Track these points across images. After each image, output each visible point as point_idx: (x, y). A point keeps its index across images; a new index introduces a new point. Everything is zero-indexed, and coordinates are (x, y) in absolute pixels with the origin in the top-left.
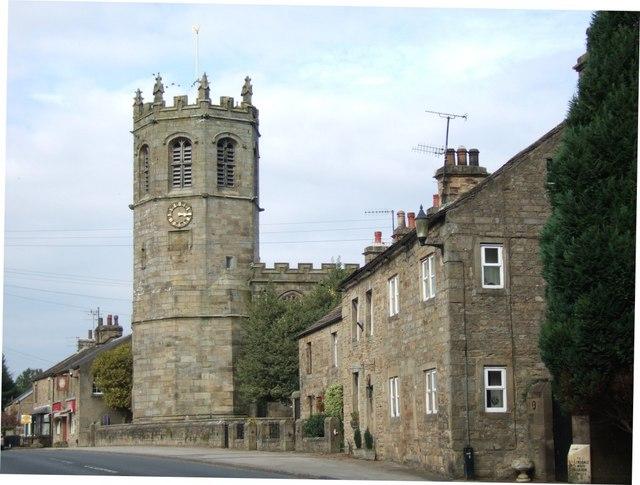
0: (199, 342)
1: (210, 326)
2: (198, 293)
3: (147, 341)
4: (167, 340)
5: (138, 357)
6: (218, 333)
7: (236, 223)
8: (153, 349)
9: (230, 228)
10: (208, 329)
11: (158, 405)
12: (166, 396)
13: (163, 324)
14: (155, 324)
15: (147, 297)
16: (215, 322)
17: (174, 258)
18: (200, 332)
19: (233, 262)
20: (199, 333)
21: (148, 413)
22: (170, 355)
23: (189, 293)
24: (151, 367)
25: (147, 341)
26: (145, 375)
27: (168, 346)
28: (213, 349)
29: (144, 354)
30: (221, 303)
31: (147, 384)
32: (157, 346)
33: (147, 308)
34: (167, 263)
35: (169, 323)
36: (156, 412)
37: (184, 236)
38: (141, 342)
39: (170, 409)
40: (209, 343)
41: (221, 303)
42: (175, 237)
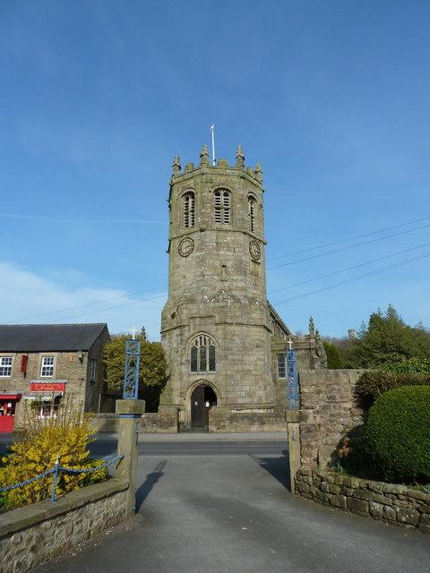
8: (244, 348)
11: (250, 395)
12: (257, 387)
15: (237, 305)
21: (240, 401)
24: (242, 362)
25: (237, 340)
26: (236, 367)
29: (235, 351)
31: (239, 376)
32: (247, 345)
33: (238, 314)
35: (258, 329)
36: (248, 400)
39: (260, 398)
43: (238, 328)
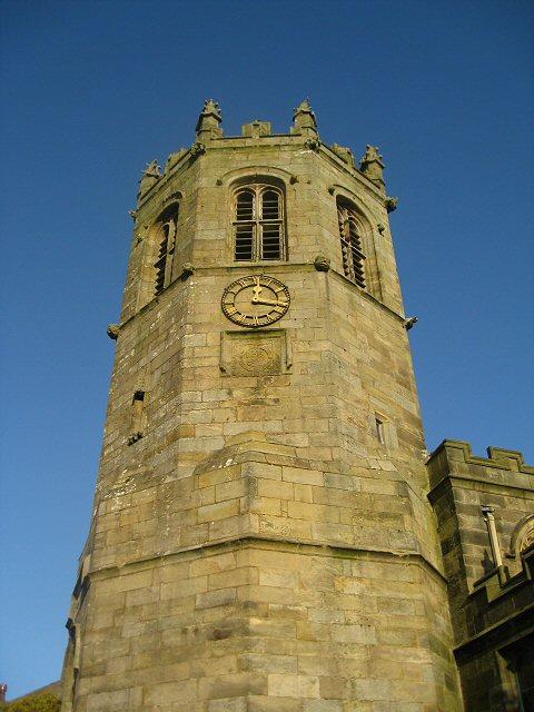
0: (328, 630)
1: (357, 582)
2: (315, 478)
3: (133, 629)
4: (218, 615)
5: (97, 682)
6: (386, 604)
7: (385, 352)
9: (375, 355)
10: (353, 588)
13: (197, 567)
14: (167, 569)
15: (148, 495)
16: (372, 569)
17: (237, 393)
18: (330, 594)
19: (388, 429)
20: (329, 602)
22: (223, 668)
23: (291, 475)
25: (133, 629)
27: (218, 636)
28: (373, 654)
29: (118, 669)
30: (384, 516)
32: (174, 639)
33: (143, 528)
34: (218, 405)
37: (268, 344)
38: (113, 632)
40: (362, 636)
41: (384, 516)
42: (243, 347)
43: (141, 580)
